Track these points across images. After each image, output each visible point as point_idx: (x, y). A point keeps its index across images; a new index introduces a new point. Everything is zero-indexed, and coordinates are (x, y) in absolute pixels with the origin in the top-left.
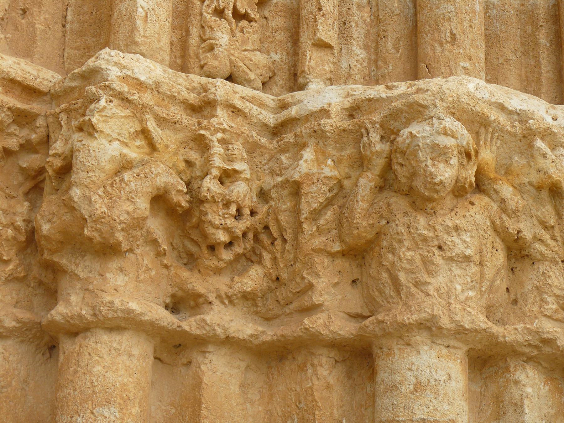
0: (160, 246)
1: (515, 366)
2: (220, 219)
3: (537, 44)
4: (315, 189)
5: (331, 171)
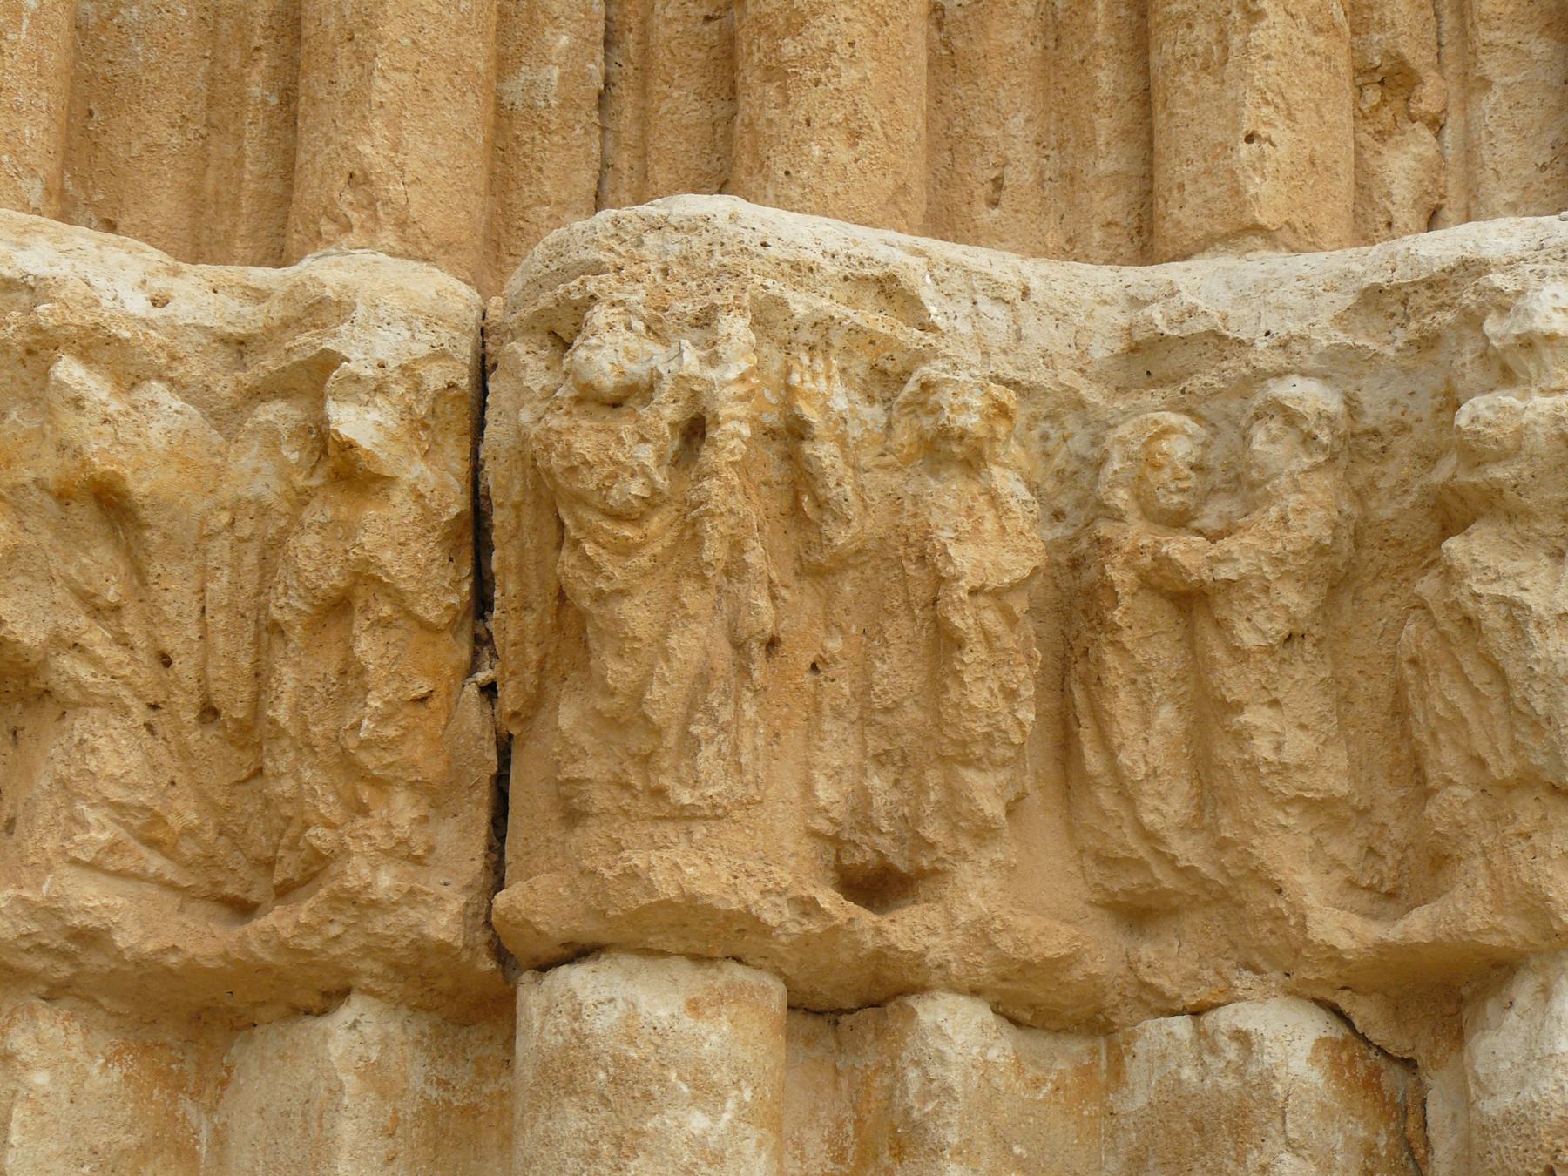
1: (11, 1014)
3: (243, 101)
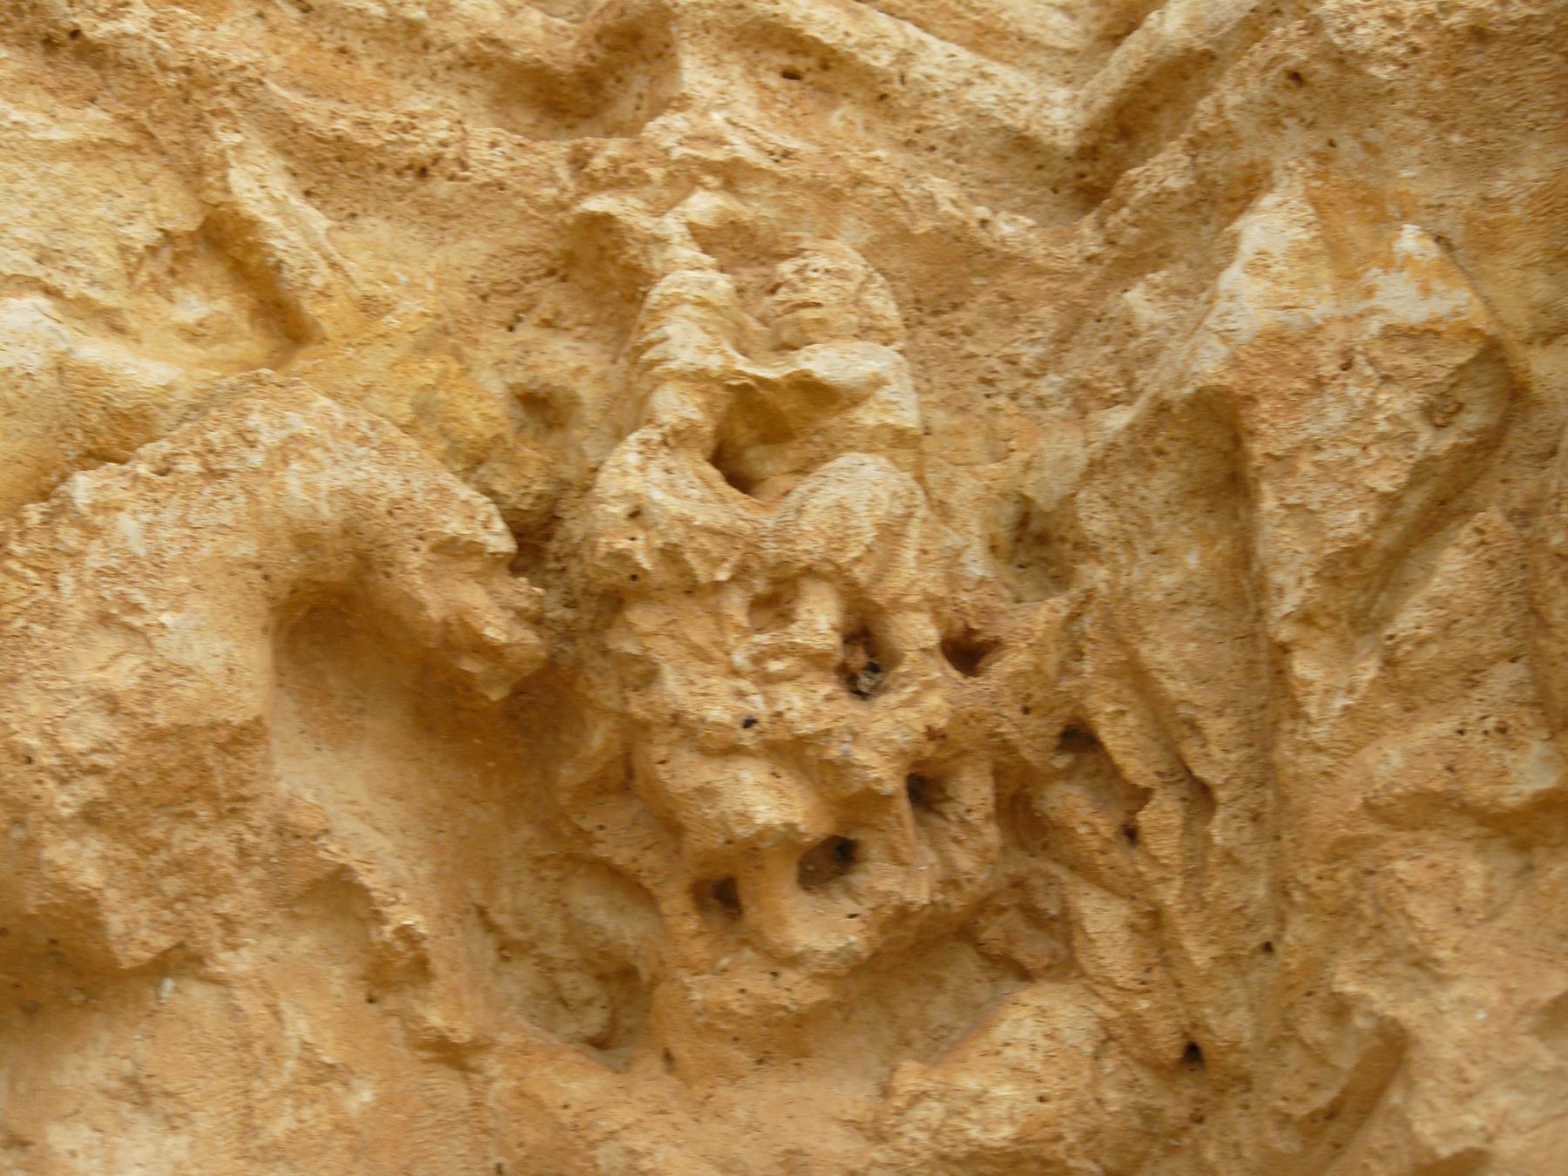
0: (379, 918)
2: (741, 695)
4: (1336, 416)
5: (1426, 291)
